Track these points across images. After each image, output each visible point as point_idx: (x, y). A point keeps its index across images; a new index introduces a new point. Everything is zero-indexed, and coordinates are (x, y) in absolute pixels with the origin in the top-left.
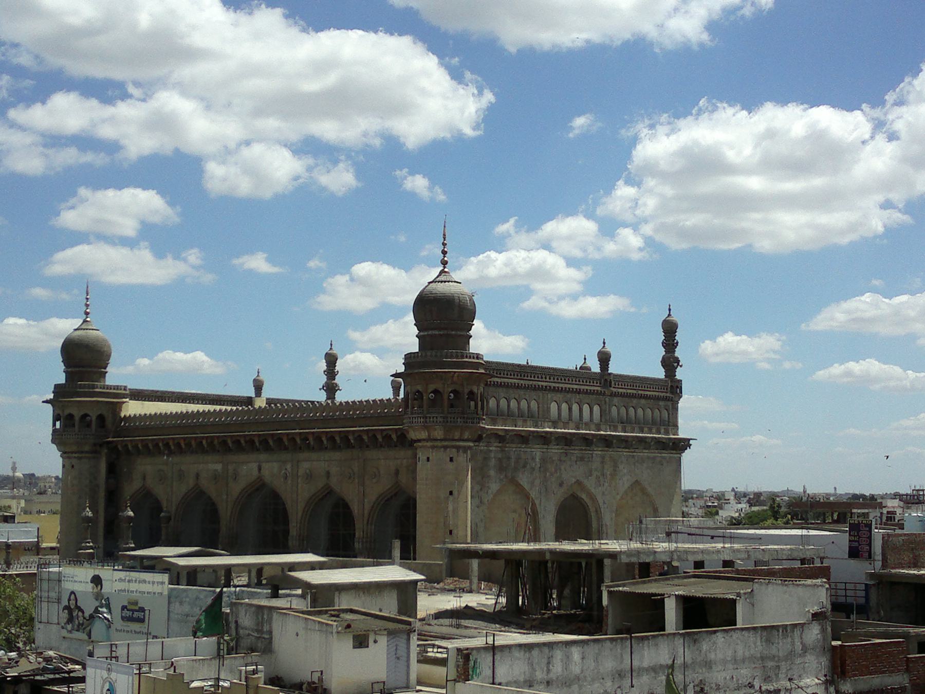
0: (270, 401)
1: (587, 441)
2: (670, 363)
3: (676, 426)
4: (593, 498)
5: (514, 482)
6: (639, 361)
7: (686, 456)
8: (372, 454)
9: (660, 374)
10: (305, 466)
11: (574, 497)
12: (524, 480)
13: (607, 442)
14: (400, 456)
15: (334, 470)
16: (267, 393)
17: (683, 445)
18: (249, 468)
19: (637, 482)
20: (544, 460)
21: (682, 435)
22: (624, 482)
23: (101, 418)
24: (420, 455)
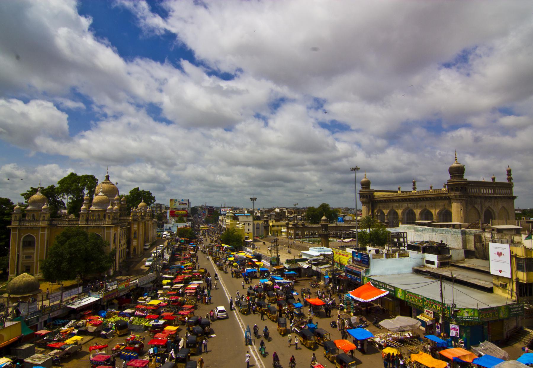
0: (402, 192)
1: (491, 197)
2: (509, 179)
3: (511, 193)
4: (493, 210)
5: (474, 207)
6: (502, 179)
7: (515, 201)
8: (437, 202)
9: (507, 181)
10: (419, 204)
11: (488, 210)
12: (476, 206)
13: (496, 197)
14: (446, 202)
15: (427, 205)
16: (401, 190)
17: (515, 197)
18: (405, 205)
19: (503, 207)
20: (481, 202)
21: (514, 195)
22: (500, 207)
23: (370, 196)
24: (452, 201)
